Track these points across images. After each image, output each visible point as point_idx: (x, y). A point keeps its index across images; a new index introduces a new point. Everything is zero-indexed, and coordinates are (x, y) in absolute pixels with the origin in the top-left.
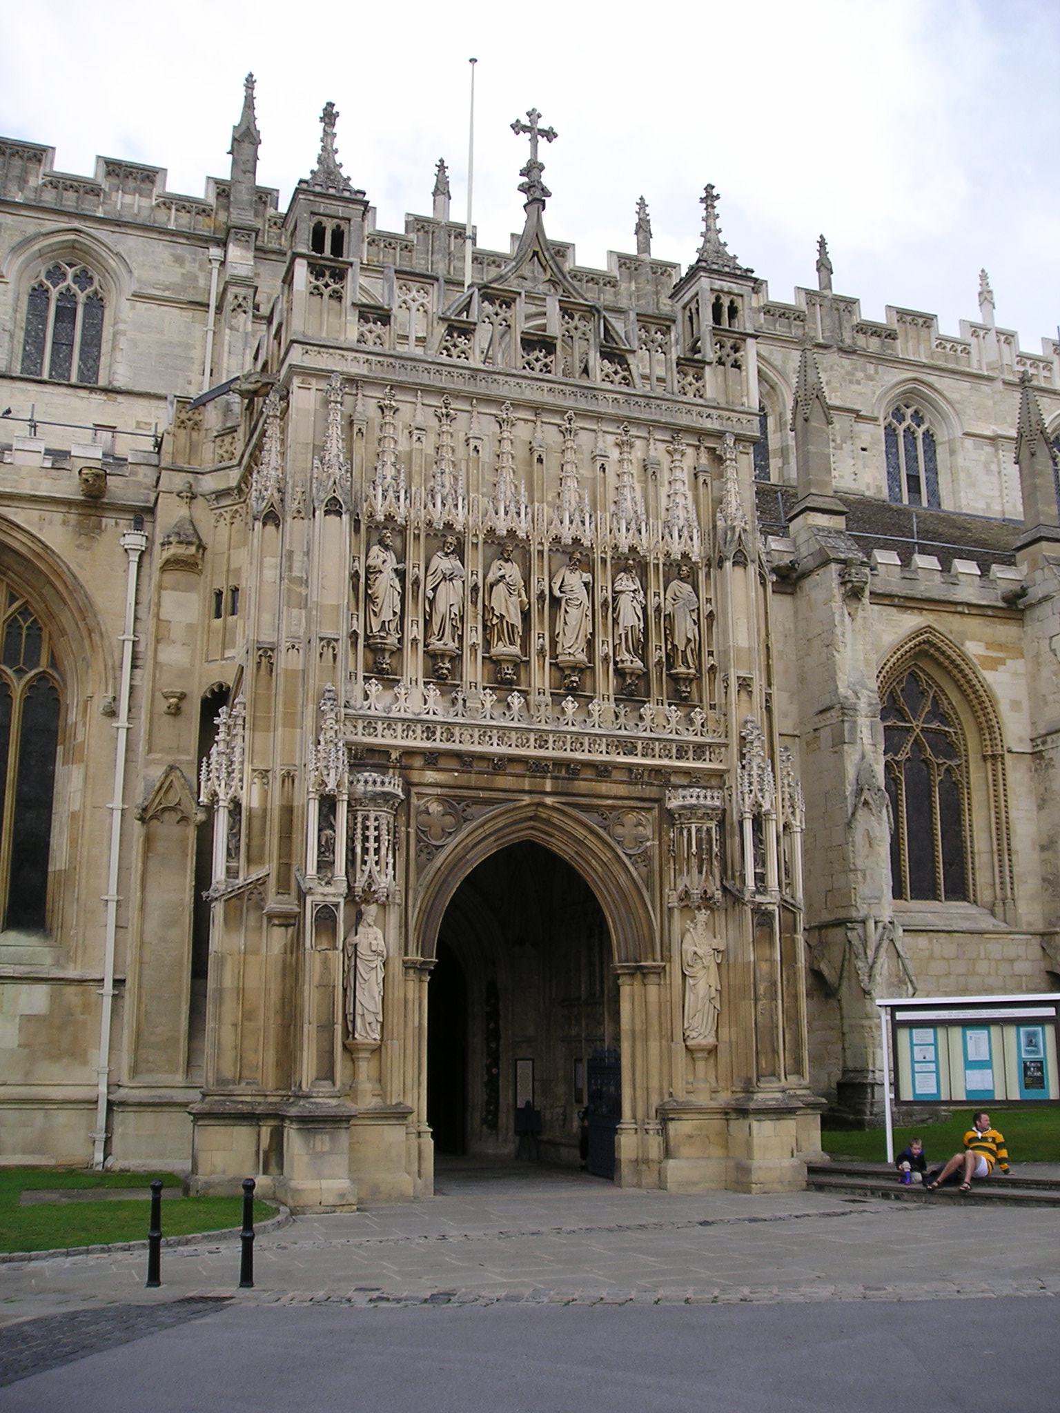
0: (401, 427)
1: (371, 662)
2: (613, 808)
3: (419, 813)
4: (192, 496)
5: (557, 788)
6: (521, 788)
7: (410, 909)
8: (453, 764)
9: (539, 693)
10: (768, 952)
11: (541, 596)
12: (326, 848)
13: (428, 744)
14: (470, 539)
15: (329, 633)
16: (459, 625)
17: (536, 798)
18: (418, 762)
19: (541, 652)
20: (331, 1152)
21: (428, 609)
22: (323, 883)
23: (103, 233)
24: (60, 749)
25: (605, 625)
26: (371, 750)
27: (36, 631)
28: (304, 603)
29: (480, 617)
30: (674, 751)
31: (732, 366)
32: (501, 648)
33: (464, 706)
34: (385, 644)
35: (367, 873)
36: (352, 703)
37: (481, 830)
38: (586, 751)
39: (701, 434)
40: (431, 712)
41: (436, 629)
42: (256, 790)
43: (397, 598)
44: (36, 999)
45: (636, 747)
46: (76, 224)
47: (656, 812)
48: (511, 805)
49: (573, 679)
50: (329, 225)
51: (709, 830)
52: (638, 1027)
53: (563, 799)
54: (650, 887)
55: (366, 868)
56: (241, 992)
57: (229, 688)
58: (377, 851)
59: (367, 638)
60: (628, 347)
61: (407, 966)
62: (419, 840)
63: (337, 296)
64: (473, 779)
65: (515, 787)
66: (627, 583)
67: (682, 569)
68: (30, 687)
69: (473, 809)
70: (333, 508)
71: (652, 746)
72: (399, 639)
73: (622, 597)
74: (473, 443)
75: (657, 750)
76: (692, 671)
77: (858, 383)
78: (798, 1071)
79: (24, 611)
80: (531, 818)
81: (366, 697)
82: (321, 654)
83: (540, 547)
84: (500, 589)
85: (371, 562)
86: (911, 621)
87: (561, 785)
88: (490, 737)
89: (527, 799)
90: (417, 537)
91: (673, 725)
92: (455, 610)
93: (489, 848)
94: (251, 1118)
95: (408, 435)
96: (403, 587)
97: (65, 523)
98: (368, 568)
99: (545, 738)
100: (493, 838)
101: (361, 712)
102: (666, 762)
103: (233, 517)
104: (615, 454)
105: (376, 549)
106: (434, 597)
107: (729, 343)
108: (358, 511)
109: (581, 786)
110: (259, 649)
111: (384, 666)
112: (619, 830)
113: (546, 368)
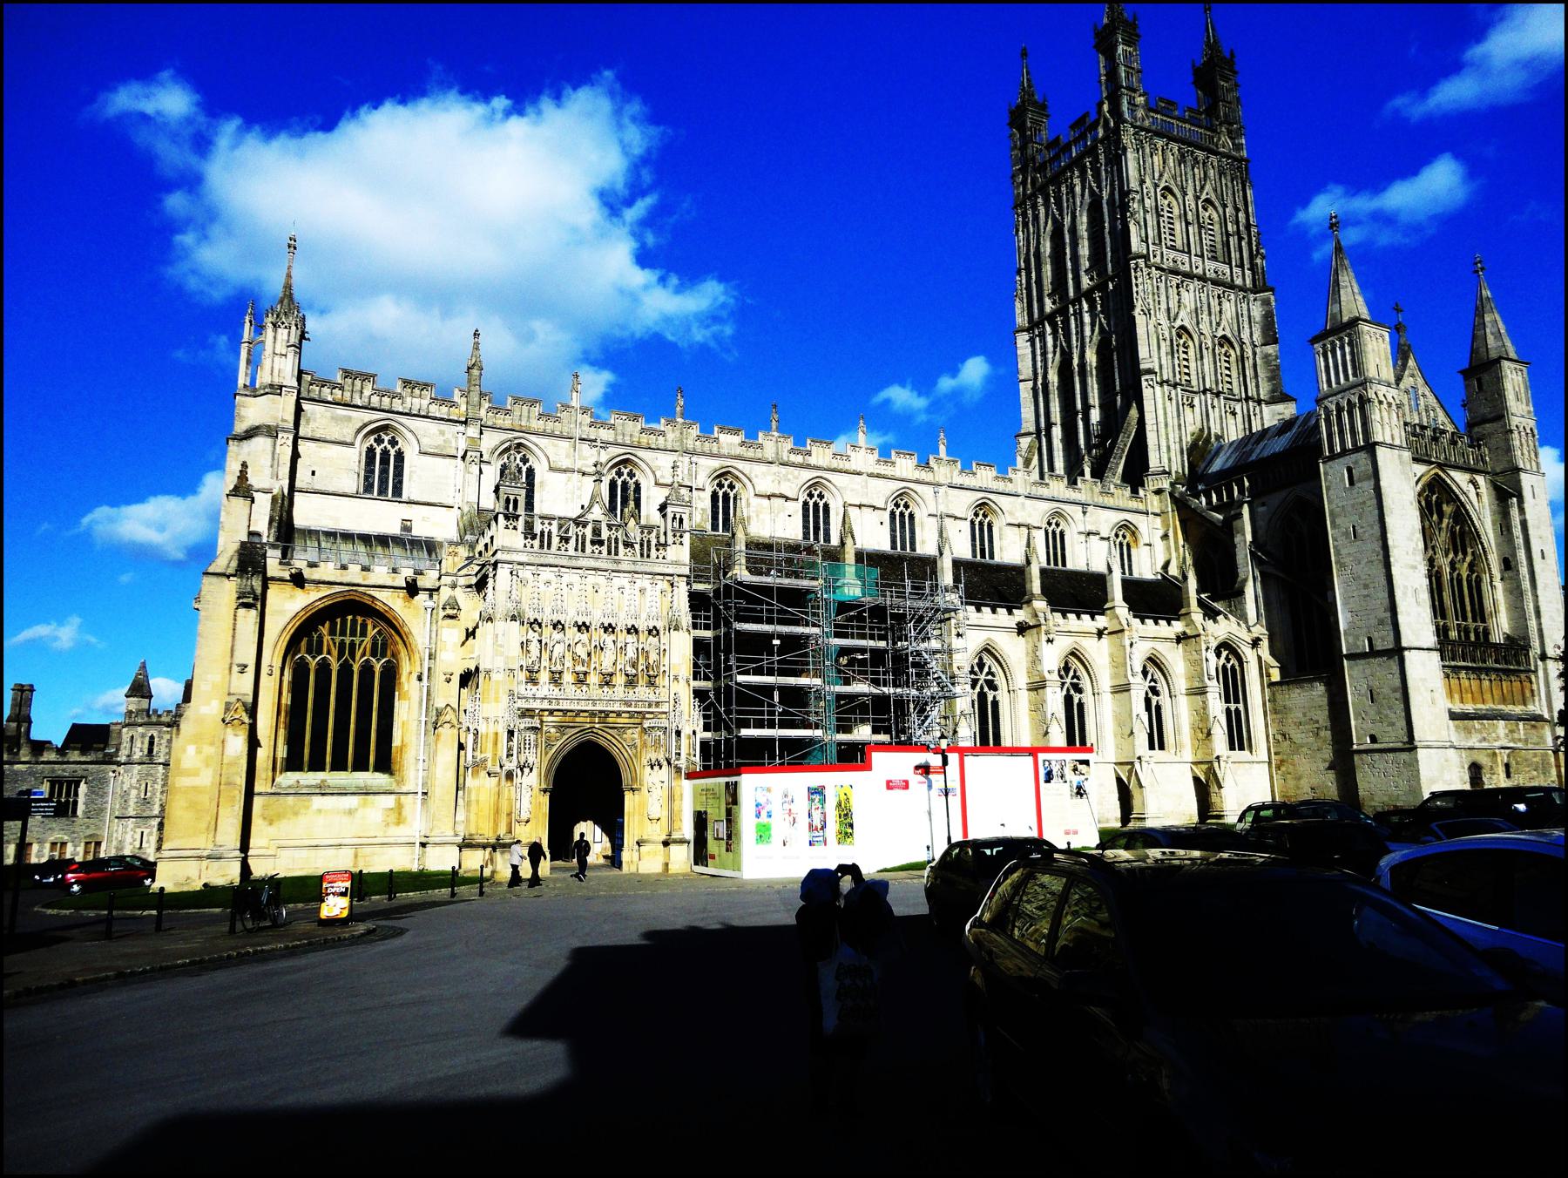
4: (454, 586)
8: (561, 714)
11: (596, 646)
12: (510, 749)
15: (511, 667)
18: (546, 713)
19: (595, 668)
23: (402, 419)
24: (397, 693)
26: (528, 710)
28: (502, 654)
32: (579, 668)
44: (390, 801)
50: (512, 498)
54: (636, 757)
56: (478, 801)
63: (515, 528)
64: (567, 719)
66: (631, 638)
67: (653, 632)
68: (383, 666)
70: (513, 618)
77: (789, 480)
79: (379, 633)
89: (588, 726)
93: (575, 744)
94: (484, 847)
102: (643, 709)
104: (627, 586)
107: (678, 534)
109: (610, 720)
113: (600, 552)
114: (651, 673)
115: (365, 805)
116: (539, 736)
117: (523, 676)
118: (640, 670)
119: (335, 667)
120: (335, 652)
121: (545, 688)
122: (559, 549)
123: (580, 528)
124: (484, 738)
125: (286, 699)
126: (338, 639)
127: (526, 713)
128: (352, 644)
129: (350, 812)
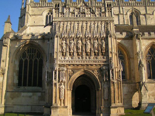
13: (69, 63)
16: (73, 49)
17: (84, 69)
20: (56, 111)
26: (62, 65)
27: (40, 54)
42: (50, 70)
44: (39, 94)
46: (50, 8)
52: (98, 97)
53: (87, 69)
55: (61, 79)
58: (63, 76)
59: (62, 51)
61: (68, 90)
64: (75, 67)
69: (76, 71)
77: (150, 10)
78: (121, 103)
86: (150, 41)
87: (87, 67)
96: (66, 45)
97: (41, 42)
102: (101, 63)
109: (90, 67)
115: (34, 95)
117: (60, 54)
119: (29, 61)
120: (28, 57)
121: (68, 58)
124: (50, 74)
125: (17, 69)
126: (29, 54)
127: (60, 65)
128: (33, 55)
129: (30, 97)
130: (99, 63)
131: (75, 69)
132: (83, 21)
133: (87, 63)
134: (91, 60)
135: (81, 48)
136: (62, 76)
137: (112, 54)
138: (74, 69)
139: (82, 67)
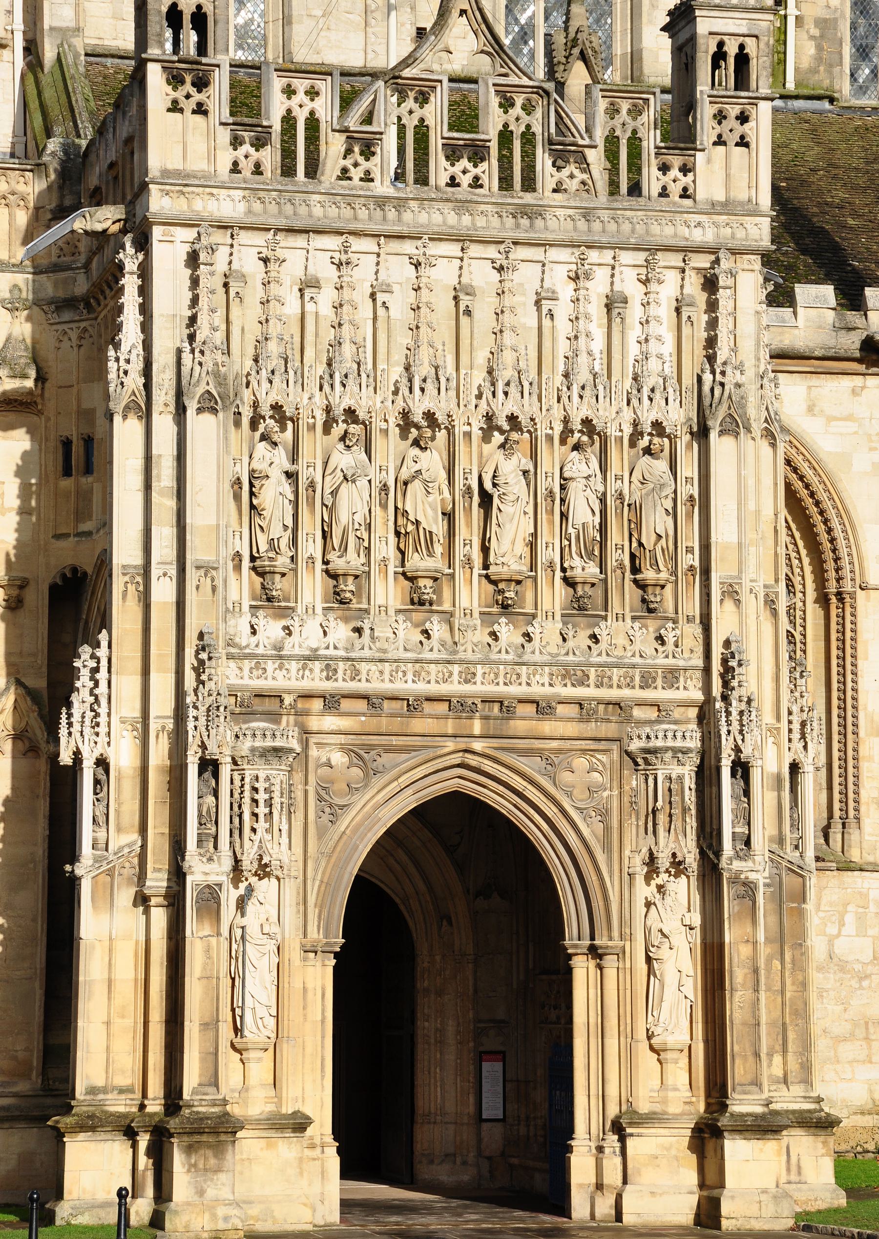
0: (289, 283)
1: (259, 587)
2: (559, 751)
3: (319, 766)
5: (489, 729)
6: (443, 732)
7: (309, 883)
8: (361, 705)
9: (465, 614)
10: (749, 929)
13: (328, 686)
14: (378, 424)
16: (365, 536)
17: (462, 743)
21: (326, 518)
22: (205, 860)
25: (551, 522)
29: (391, 524)
30: (637, 679)
31: (737, 145)
33: (372, 638)
34: (275, 566)
35: (257, 843)
36: (237, 640)
37: (395, 783)
38: (524, 683)
39: (686, 250)
40: (331, 647)
41: (336, 542)
43: (289, 510)
45: (588, 676)
47: (616, 755)
48: (431, 753)
49: (507, 595)
51: (680, 778)
53: (495, 743)
54: (607, 847)
57: (85, 574)
59: (253, 559)
60: (587, 142)
62: (320, 799)
64: (384, 723)
65: (436, 731)
69: (386, 759)
71: (609, 673)
72: (292, 557)
73: (572, 485)
74: (380, 297)
75: (615, 679)
76: (664, 575)
80: (458, 766)
81: (254, 632)
82: (198, 587)
83: (467, 428)
84: (416, 487)
85: (255, 465)
88: (404, 673)
89: (450, 745)
90: (312, 428)
91: (637, 646)
92: (359, 518)
95: (299, 294)
96: (296, 493)
98: (252, 473)
99: (473, 670)
100: (409, 791)
101: (247, 651)
102: (626, 693)
103: (81, 338)
104: (566, 291)
105: (262, 448)
106: (334, 503)
108: (238, 402)
109: (518, 726)
110: (124, 574)
111: (274, 593)
112: (566, 777)
114: (648, 575)
116: (298, 777)
118: (611, 562)
122: (344, 174)
123: (410, 103)
130: (614, 694)
131: (383, 740)
132: (463, 239)
133: (501, 689)
134: (537, 658)
135: (439, 528)
136: (262, 810)
137: (738, 602)
138: (375, 740)
139: (450, 727)
